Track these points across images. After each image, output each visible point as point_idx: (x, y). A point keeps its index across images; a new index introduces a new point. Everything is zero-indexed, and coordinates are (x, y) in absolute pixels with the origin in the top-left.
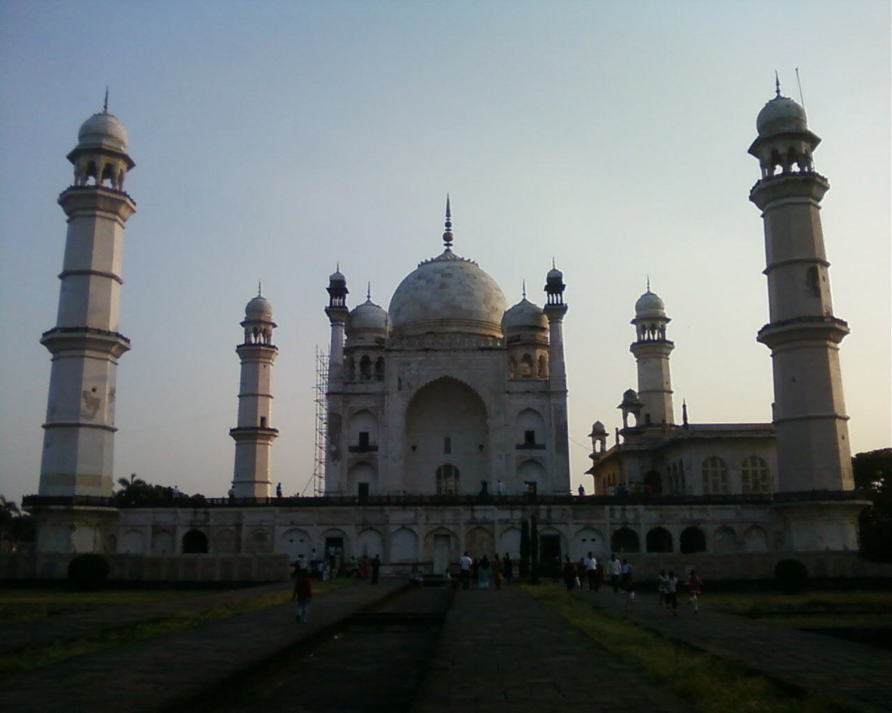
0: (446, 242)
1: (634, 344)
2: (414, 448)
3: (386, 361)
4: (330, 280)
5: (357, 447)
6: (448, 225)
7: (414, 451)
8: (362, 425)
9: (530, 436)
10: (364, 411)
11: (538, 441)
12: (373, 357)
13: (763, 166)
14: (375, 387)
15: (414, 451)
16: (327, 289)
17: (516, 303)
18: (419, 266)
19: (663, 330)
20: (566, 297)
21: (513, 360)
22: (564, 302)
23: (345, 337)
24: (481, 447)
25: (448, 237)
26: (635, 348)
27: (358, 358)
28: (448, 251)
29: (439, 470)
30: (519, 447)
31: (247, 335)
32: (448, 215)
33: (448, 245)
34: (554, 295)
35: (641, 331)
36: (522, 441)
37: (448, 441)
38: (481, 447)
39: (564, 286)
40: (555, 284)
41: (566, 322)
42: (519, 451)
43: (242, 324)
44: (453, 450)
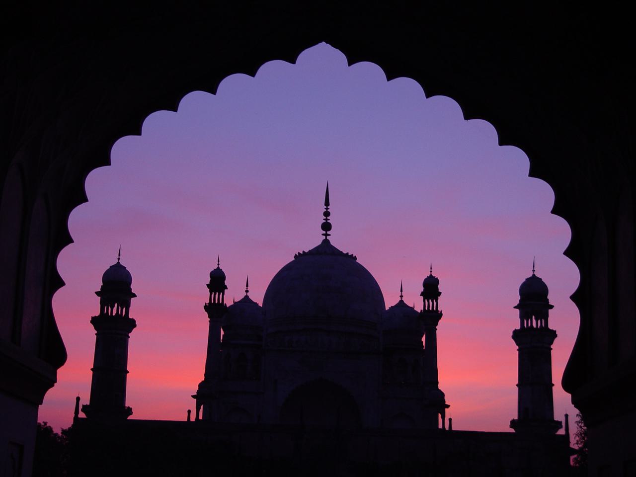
0: (324, 232)
1: (515, 332)
6: (327, 214)
16: (207, 285)
17: (393, 305)
18: (296, 256)
20: (443, 304)
22: (439, 309)
25: (326, 227)
26: (517, 336)
28: (326, 242)
31: (103, 304)
32: (327, 203)
33: (326, 235)
34: (430, 300)
35: (524, 316)
39: (441, 293)
41: (442, 328)
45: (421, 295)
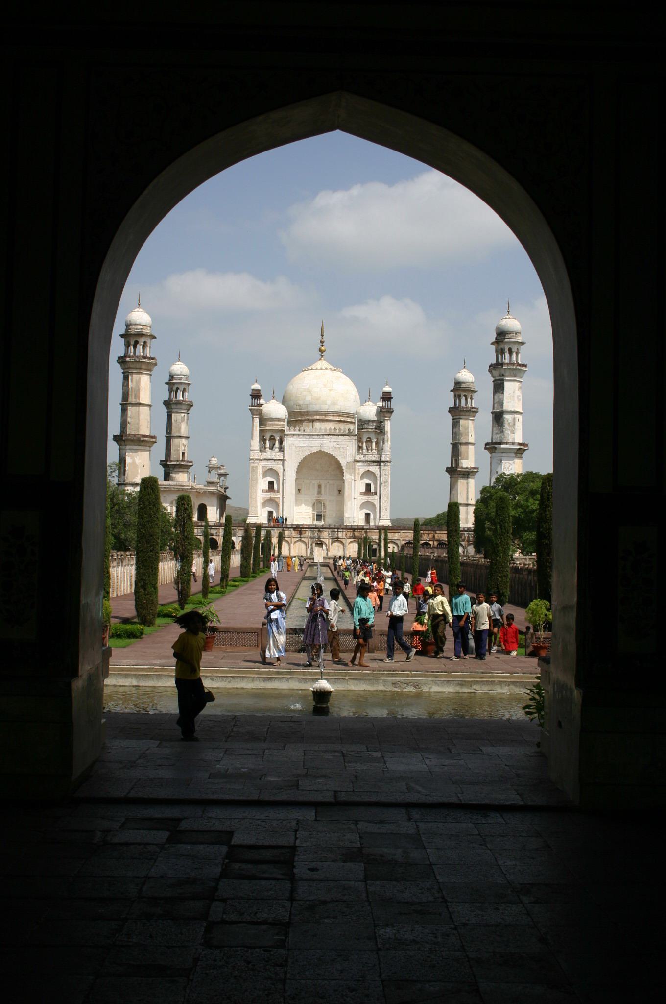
10: (271, 469)
11: (373, 490)
13: (496, 351)
14: (279, 456)
19: (471, 398)
21: (360, 440)
24: (340, 491)
27: (268, 436)
29: (314, 505)
30: (361, 493)
32: (322, 335)
35: (457, 397)
36: (363, 489)
37: (320, 486)
38: (340, 491)
44: (323, 492)
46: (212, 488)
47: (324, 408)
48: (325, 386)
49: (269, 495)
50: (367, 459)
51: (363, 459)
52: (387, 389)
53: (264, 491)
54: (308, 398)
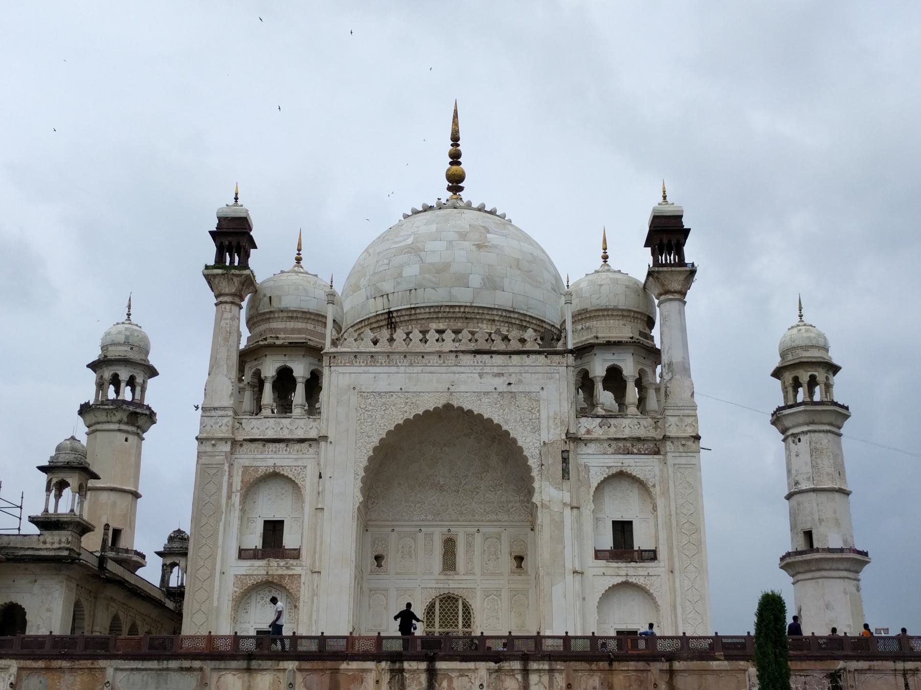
2: (379, 558)
3: (326, 371)
4: (219, 219)
5: (256, 549)
7: (379, 566)
8: (270, 505)
9: (623, 529)
10: (274, 476)
11: (641, 540)
12: (300, 370)
15: (379, 566)
20: (691, 251)
23: (245, 333)
24: (520, 559)
25: (455, 182)
27: (269, 368)
30: (598, 555)
36: (607, 543)
37: (449, 545)
38: (520, 559)
40: (667, 234)
42: (602, 563)
43: (94, 366)
45: (646, 246)
46: (56, 541)
47: (463, 296)
48: (463, 236)
49: (258, 568)
50: (612, 433)
51: (598, 433)
52: (668, 210)
53: (243, 554)
54: (412, 271)
